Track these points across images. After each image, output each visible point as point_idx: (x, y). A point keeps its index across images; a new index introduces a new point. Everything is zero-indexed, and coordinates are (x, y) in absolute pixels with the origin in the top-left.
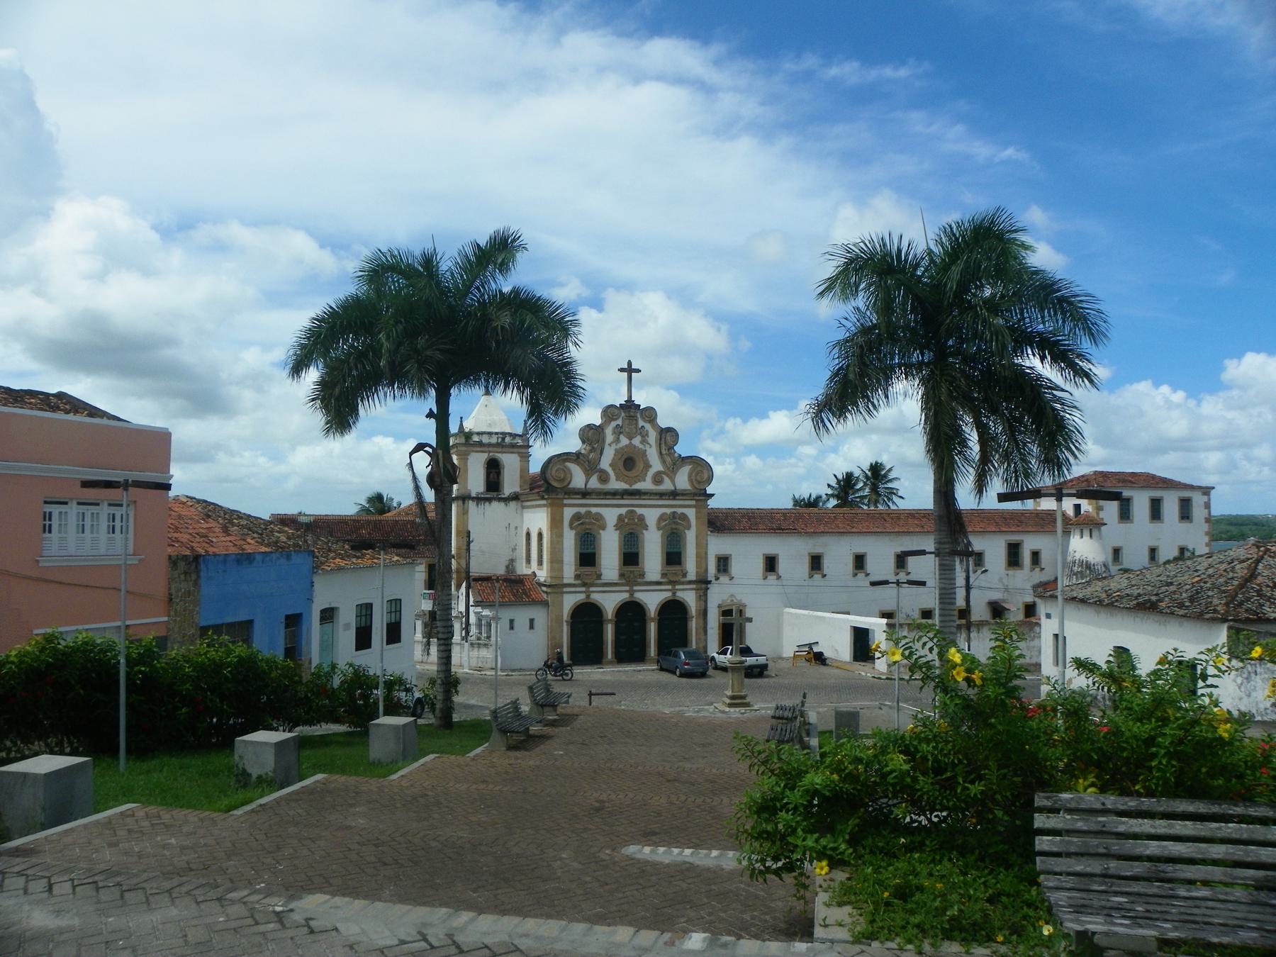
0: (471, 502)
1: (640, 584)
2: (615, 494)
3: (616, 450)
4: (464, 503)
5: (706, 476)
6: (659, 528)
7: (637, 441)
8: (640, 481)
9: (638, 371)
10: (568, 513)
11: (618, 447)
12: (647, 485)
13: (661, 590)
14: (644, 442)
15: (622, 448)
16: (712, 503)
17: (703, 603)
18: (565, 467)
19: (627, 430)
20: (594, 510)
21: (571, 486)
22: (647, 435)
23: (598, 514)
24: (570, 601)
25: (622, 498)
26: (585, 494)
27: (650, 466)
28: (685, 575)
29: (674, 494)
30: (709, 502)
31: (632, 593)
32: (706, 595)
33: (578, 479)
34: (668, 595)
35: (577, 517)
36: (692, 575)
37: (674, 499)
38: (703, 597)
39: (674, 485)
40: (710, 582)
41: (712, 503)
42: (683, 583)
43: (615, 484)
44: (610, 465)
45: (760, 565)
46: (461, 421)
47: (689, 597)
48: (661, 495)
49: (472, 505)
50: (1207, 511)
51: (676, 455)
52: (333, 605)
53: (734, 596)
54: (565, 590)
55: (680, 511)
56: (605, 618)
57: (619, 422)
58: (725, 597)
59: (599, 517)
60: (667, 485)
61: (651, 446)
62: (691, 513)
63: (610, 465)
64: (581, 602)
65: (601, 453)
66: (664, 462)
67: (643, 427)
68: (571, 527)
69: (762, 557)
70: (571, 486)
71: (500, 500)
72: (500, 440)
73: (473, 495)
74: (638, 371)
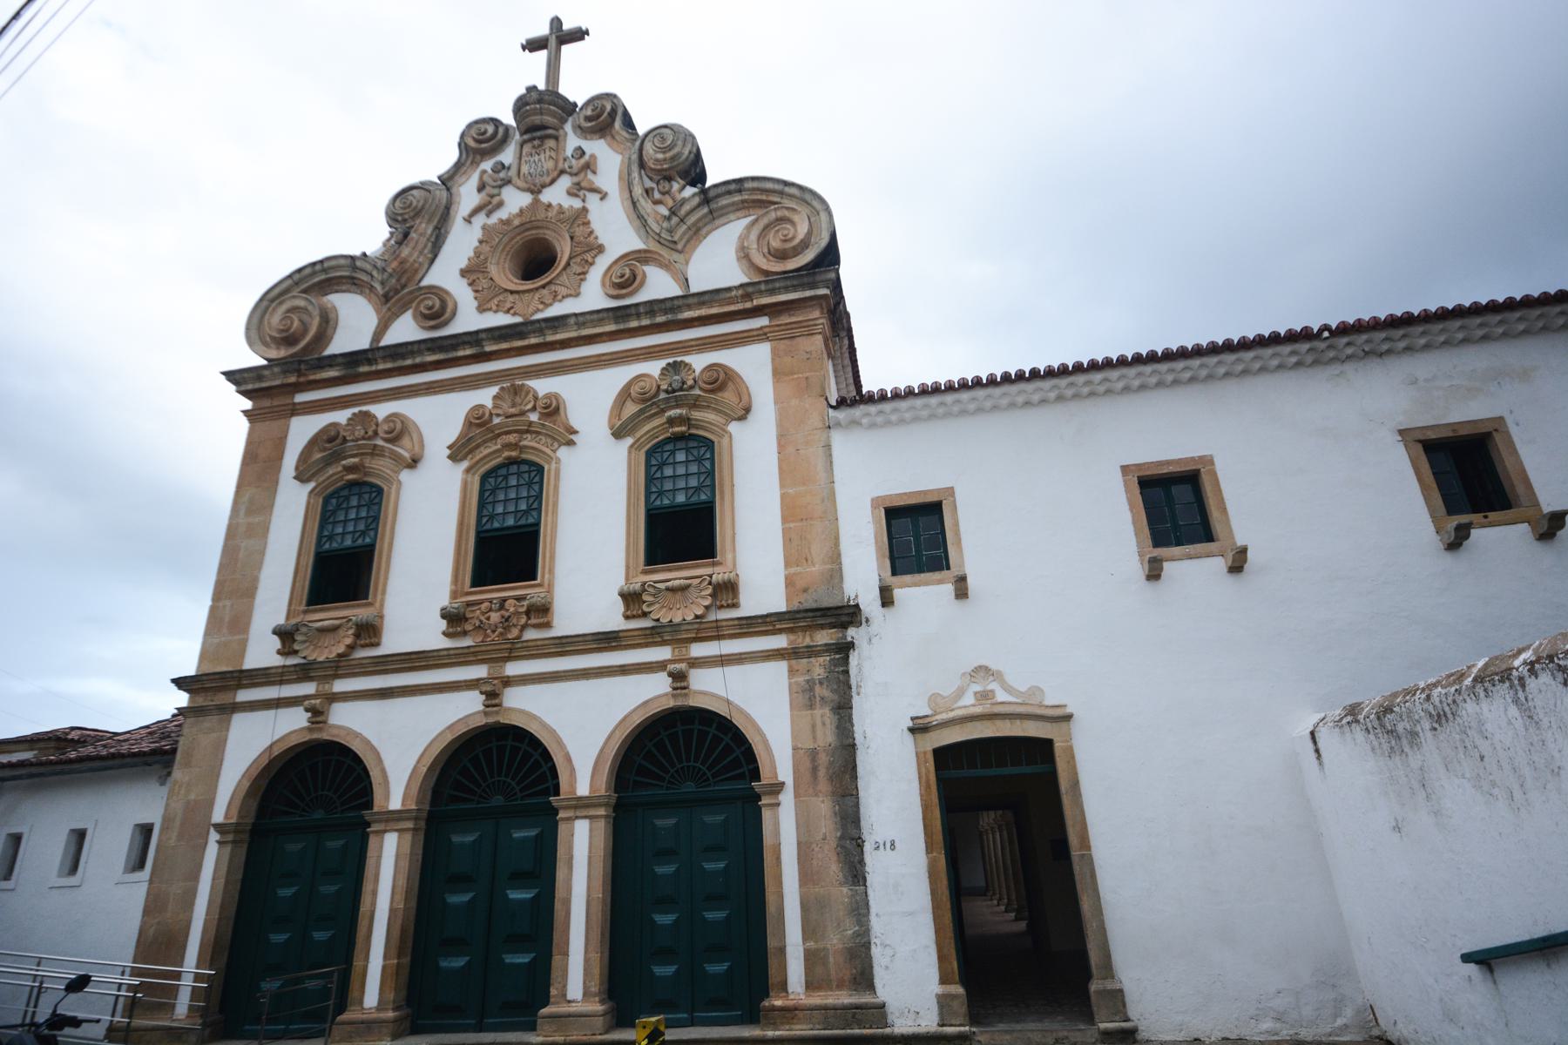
3: (484, 228)
7: (557, 195)
9: (579, 35)
10: (302, 430)
11: (494, 219)
13: (624, 670)
17: (824, 715)
22: (590, 166)
28: (727, 591)
35: (329, 440)
43: (469, 318)
44: (464, 273)
54: (244, 696)
59: (400, 430)
61: (604, 196)
63: (464, 273)
64: (294, 741)
69: (1117, 480)
74: (579, 35)
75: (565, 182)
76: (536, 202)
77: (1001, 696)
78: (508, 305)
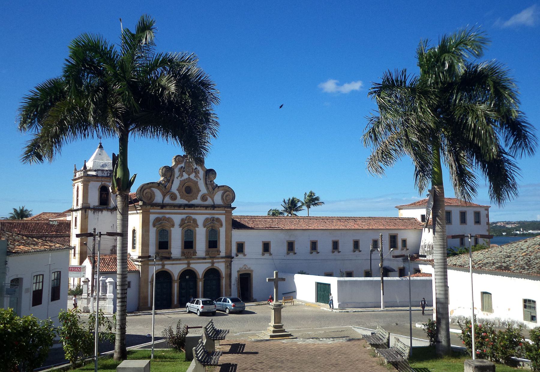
0: (90, 211)
1: (194, 259)
2: (180, 206)
4: (85, 212)
5: (231, 197)
6: (205, 226)
7: (192, 176)
8: (194, 199)
10: (152, 217)
12: (197, 201)
13: (206, 263)
14: (196, 176)
15: (184, 180)
16: (235, 213)
17: (229, 270)
18: (152, 191)
19: (187, 170)
20: (167, 216)
21: (154, 202)
23: (169, 218)
24: (153, 270)
25: (184, 209)
26: (163, 206)
27: (200, 191)
29: (214, 207)
30: (233, 212)
31: (189, 264)
32: (230, 265)
33: (158, 197)
34: (208, 266)
35: (157, 220)
36: (223, 254)
37: (214, 210)
38: (229, 266)
39: (214, 202)
40: (233, 258)
41: (235, 213)
42: (218, 258)
43: (180, 201)
44: (177, 190)
45: (260, 248)
46: (85, 163)
47: (221, 266)
48: (206, 207)
49: (90, 213)
50: (487, 218)
51: (215, 185)
52: (19, 277)
53: (247, 266)
55: (216, 216)
56: (173, 279)
57: (183, 165)
58: (241, 266)
59: (170, 220)
60: (209, 202)
62: (223, 218)
63: (177, 190)
64: (160, 270)
65: (172, 183)
66: (208, 189)
67: (196, 168)
68: (154, 225)
70: (154, 202)
71: (108, 209)
72: (109, 175)
73: (91, 206)
75: (194, 174)
76: (189, 177)
77: (247, 268)
78: (186, 199)
